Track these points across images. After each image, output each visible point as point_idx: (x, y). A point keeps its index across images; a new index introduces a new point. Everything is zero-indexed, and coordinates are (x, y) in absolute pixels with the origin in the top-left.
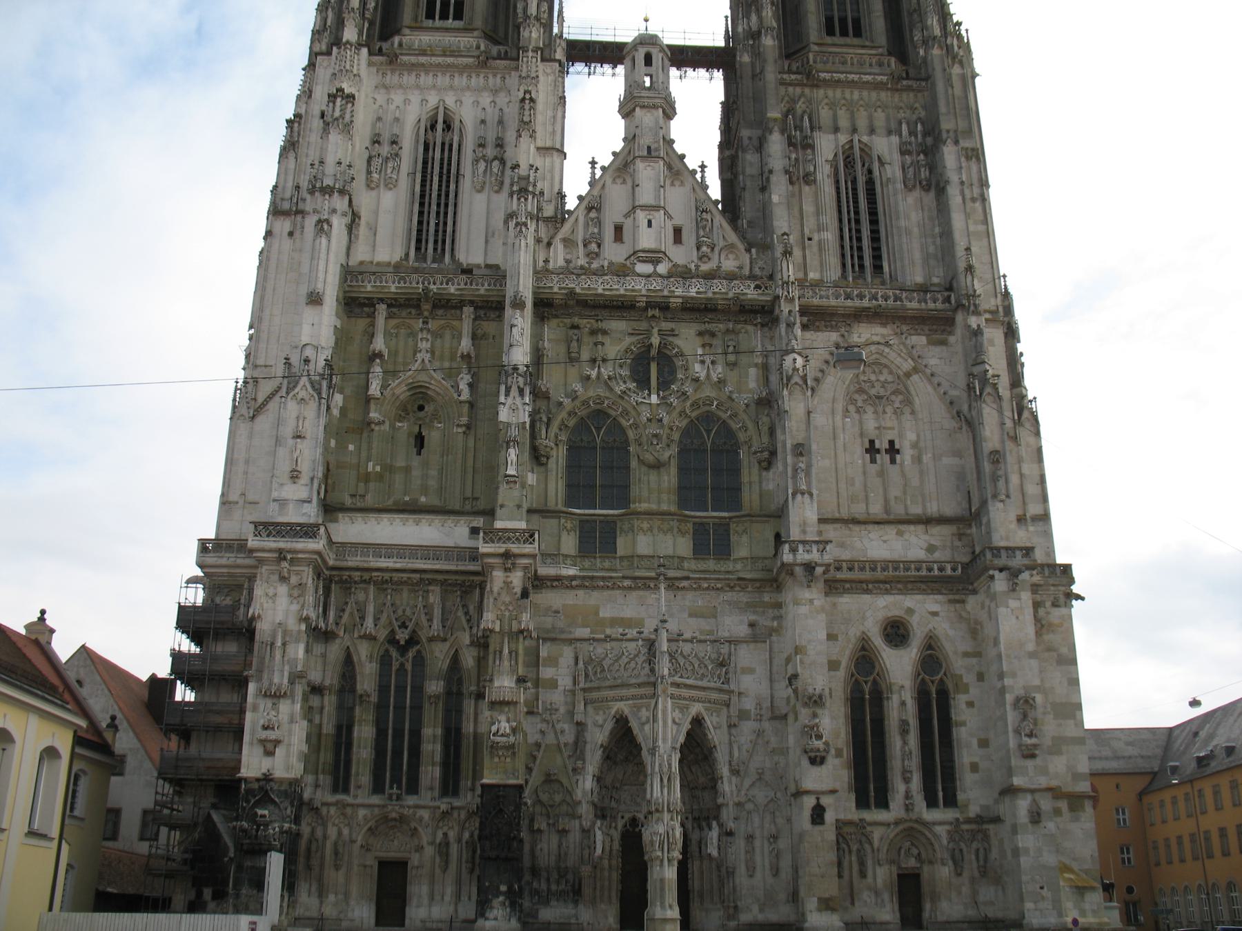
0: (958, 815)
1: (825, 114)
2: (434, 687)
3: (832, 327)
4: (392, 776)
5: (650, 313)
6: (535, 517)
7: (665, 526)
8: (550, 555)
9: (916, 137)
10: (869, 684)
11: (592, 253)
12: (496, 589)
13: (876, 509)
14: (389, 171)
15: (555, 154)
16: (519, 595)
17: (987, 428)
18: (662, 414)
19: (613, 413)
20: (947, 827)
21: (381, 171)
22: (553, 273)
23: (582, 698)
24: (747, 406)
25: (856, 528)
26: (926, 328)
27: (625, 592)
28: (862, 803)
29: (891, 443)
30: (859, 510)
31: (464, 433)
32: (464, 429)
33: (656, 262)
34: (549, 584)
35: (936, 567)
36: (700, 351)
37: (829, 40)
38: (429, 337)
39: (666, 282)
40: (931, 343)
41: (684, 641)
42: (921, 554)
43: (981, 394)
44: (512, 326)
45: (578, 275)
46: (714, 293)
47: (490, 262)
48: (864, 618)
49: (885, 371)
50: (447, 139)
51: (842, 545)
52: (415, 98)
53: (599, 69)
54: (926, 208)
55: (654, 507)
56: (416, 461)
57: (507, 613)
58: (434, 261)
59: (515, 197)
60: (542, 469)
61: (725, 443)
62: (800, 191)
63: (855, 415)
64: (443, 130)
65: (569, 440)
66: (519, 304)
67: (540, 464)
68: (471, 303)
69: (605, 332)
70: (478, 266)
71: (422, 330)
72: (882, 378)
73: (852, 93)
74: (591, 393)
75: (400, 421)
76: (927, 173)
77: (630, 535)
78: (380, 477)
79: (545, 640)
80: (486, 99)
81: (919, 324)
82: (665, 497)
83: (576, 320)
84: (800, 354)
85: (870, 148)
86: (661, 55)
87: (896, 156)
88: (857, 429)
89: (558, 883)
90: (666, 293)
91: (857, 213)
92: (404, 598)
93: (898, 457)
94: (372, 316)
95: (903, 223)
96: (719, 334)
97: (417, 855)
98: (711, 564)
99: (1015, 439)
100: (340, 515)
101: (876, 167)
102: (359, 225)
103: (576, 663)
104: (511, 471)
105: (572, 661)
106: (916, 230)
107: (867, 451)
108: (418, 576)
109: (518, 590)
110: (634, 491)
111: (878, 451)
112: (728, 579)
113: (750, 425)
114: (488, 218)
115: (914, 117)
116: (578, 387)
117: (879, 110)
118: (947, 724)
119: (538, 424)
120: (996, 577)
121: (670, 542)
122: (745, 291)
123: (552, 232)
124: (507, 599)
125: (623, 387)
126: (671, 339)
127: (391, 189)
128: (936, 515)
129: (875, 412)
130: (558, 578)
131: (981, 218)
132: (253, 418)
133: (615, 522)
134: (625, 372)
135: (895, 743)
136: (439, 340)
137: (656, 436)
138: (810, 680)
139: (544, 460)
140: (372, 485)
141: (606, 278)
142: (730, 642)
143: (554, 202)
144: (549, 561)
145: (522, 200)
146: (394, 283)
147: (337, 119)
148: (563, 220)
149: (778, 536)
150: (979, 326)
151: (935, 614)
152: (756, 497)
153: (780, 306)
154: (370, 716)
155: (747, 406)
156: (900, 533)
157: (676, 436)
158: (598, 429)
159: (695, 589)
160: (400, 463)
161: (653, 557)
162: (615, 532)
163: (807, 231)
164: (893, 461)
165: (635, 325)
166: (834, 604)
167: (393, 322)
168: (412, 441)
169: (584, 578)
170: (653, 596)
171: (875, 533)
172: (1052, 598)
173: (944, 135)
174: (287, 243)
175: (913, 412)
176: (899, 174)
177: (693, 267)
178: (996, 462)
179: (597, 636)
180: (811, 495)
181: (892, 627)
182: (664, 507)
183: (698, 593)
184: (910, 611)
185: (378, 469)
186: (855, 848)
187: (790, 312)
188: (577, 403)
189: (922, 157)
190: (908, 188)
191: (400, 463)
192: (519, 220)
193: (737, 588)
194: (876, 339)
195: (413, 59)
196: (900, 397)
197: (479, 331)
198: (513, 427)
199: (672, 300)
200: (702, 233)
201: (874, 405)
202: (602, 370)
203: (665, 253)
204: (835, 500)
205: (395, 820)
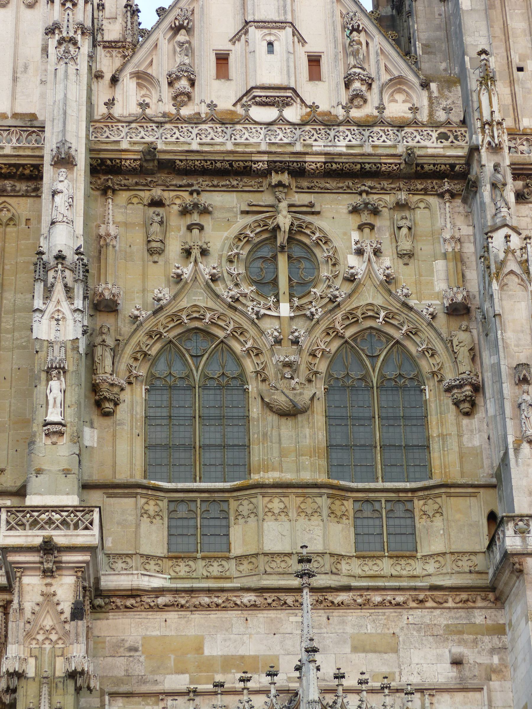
5: (275, 178)
7: (309, 506)
8: (120, 555)
11: (182, 94)
16: (67, 614)
19: (221, 334)
22: (119, 121)
24: (433, 316)
33: (285, 103)
34: (118, 601)
36: (355, 236)
39: (298, 132)
41: (347, 691)
44: (55, 193)
45: (160, 124)
47: (19, 110)
55: (289, 477)
57: (47, 646)
60: (107, 422)
67: (107, 414)
69: (205, 211)
74: (184, 303)
77: (252, 520)
79: (113, 695)
82: (306, 461)
83: (157, 192)
84: (514, 229)
90: (298, 148)
96: (385, 212)
104: (54, 416)
109: (67, 607)
112: (415, 589)
113: (439, 347)
114: (16, 45)
116: (166, 294)
119: (99, 349)
121: (318, 532)
122: (423, 143)
125: (235, 292)
126: (309, 218)
134: (239, 269)
137: (288, 365)
139: (108, 406)
141: (203, 126)
142: (422, 691)
143: (120, 20)
144: (120, 565)
148: (135, 46)
149: (492, 517)
152: (453, 457)
153: (479, 161)
157: (322, 367)
162: (227, 518)
169: (176, 591)
170: (293, 619)
177: (340, 113)
179: (201, 687)
182: (307, 477)
183: (365, 612)
187: (496, 168)
188: (162, 317)
192: (64, 34)
193: (430, 604)
197: (5, 212)
198: (56, 347)
199: (308, 159)
200: (352, 61)
202: (201, 266)
203: (294, 90)
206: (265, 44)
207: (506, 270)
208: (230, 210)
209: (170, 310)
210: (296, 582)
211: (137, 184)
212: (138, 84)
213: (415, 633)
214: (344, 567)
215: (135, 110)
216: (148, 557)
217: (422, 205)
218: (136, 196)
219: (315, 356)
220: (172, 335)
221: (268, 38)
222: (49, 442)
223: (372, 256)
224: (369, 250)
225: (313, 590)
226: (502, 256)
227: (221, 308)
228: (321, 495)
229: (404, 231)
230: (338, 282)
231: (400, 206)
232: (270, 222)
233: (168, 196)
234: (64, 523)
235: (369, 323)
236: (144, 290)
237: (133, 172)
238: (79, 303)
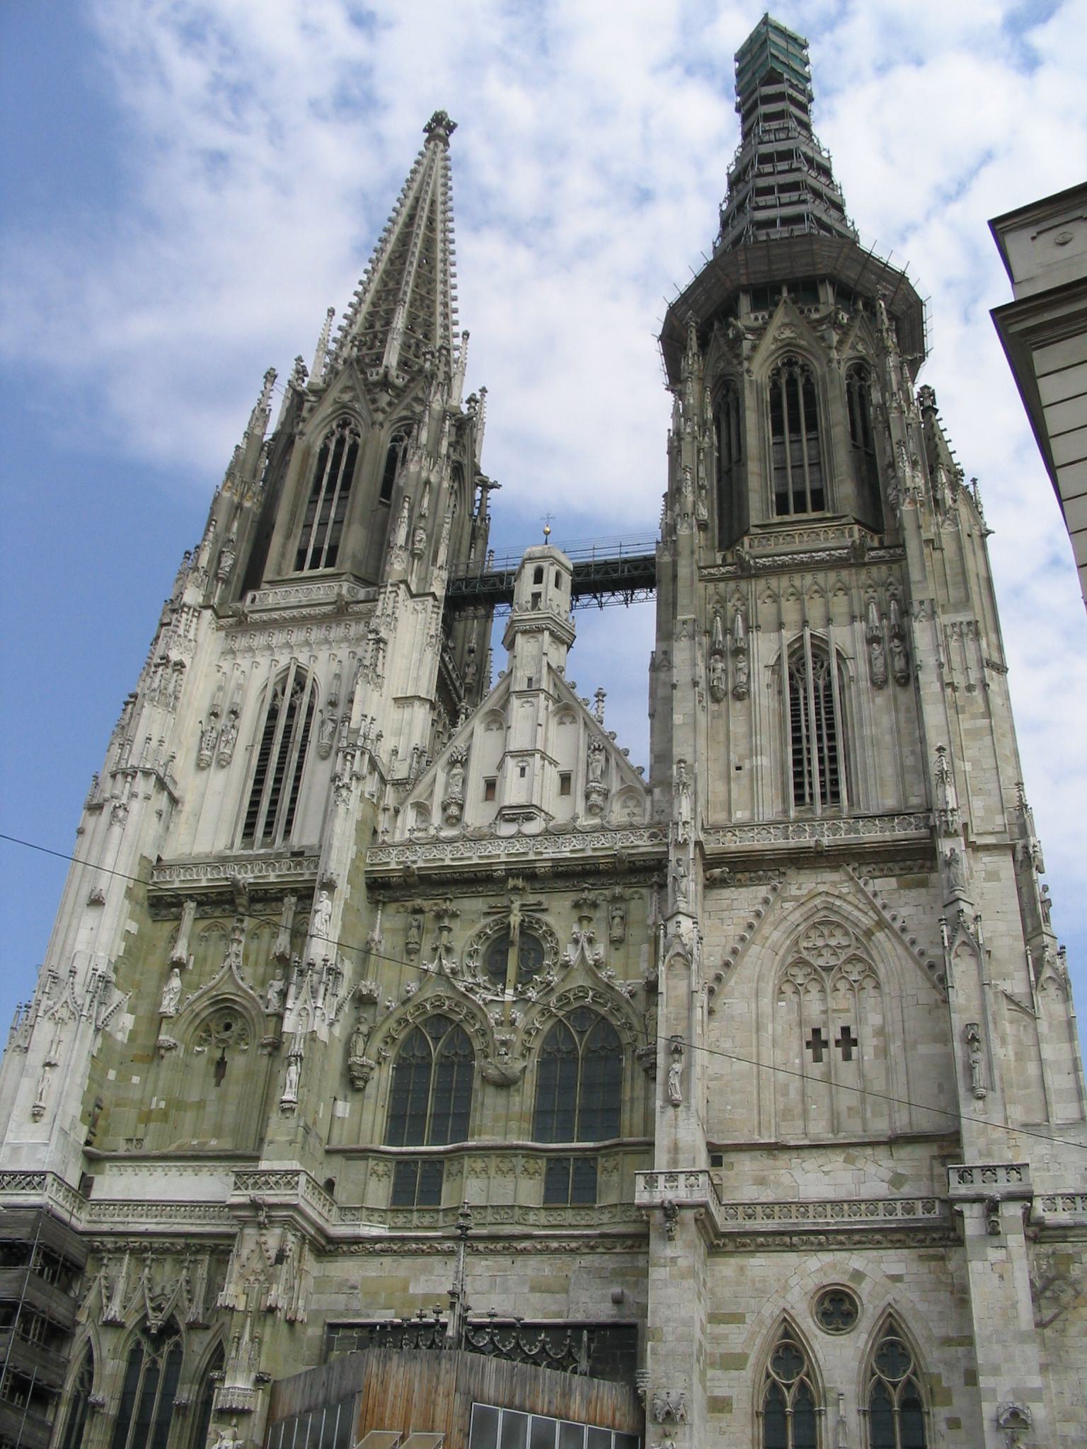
1: (765, 610)
3: (759, 879)
5: (511, 883)
6: (338, 1161)
9: (889, 619)
10: (793, 1390)
13: (819, 1129)
14: (223, 745)
15: (417, 703)
16: (273, 1260)
17: (960, 993)
18: (517, 1014)
19: (456, 1018)
21: (214, 747)
24: (633, 994)
25: (784, 1158)
27: (445, 1259)
29: (846, 1030)
31: (270, 1055)
32: (269, 1049)
33: (529, 818)
36: (576, 929)
38: (243, 939)
39: (533, 842)
40: (904, 886)
42: (882, 1190)
43: (951, 943)
46: (594, 850)
48: (786, 1288)
49: (838, 933)
51: (761, 1182)
52: (264, 660)
54: (903, 708)
58: (263, 845)
59: (340, 755)
60: (360, 1096)
61: (603, 1048)
63: (792, 996)
65: (399, 1057)
72: (833, 942)
73: (803, 579)
74: (429, 994)
75: (200, 1045)
76: (903, 662)
77: (458, 1179)
78: (164, 1115)
80: (343, 652)
81: (885, 862)
87: (861, 648)
94: (178, 918)
95: (867, 731)
98: (569, 1216)
100: (108, 1165)
102: (181, 811)
104: (289, 1096)
106: (888, 738)
107: (808, 1044)
108: (183, 1240)
109: (273, 1253)
110: (475, 1120)
111: (825, 1044)
112: (587, 1236)
116: (413, 987)
117: (841, 593)
120: (966, 1214)
122: (636, 843)
123: (403, 795)
124: (258, 1266)
126: (538, 915)
127: (223, 767)
129: (822, 991)
130: (357, 1240)
131: (982, 709)
133: (442, 1162)
134: (477, 963)
136: (255, 941)
137: (504, 1043)
139: (360, 1083)
140: (152, 1125)
143: (409, 760)
145: (349, 757)
146: (205, 875)
147: (154, 690)
150: (953, 850)
151: (897, 1278)
155: (633, 994)
157: (536, 1044)
158: (436, 1039)
159: (540, 1252)
161: (485, 1207)
163: (734, 760)
164: (847, 1057)
165: (493, 901)
166: (742, 1268)
167: (206, 922)
168: (212, 1069)
170: (483, 1263)
171: (812, 1162)
173: (916, 608)
175: (877, 986)
176: (863, 668)
178: (972, 1041)
180: (688, 1108)
181: (832, 1300)
183: (544, 1257)
184: (858, 1276)
185: (163, 1105)
189: (896, 641)
191: (194, 1097)
194: (822, 888)
195: (265, 616)
196: (860, 967)
198: (298, 1039)
201: (819, 980)
202: (444, 962)
204: (756, 1117)
206: (519, 769)
211: (404, 896)
212: (418, 812)
213: (585, 1276)
214: (532, 1218)
216: (373, 1210)
217: (636, 896)
218: (403, 906)
219: (530, 1034)
220: (417, 1021)
221: (521, 764)
223: (586, 945)
224: (583, 940)
228: (516, 1156)
229: (617, 920)
232: (505, 921)
233: (426, 904)
236: (399, 985)
237: (399, 886)
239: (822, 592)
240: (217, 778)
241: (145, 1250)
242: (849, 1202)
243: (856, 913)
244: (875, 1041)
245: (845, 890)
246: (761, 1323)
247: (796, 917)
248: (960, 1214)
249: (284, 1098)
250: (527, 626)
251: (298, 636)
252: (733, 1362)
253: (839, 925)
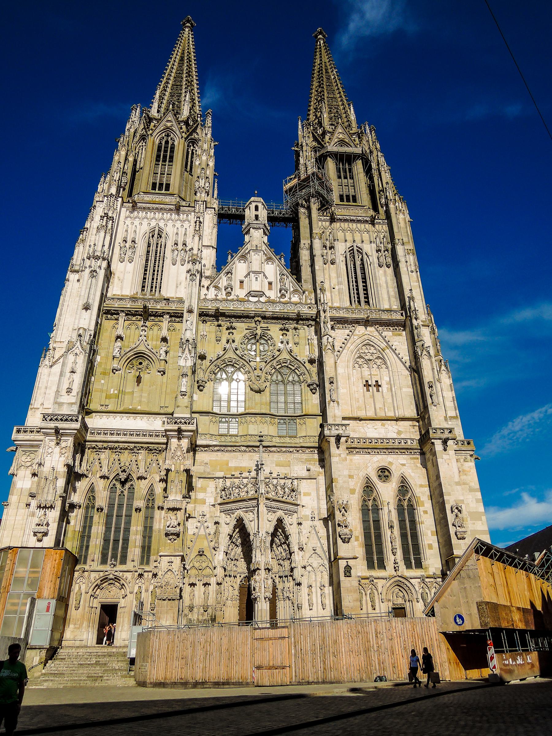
0: (423, 574)
1: (340, 235)
2: (139, 503)
4: (112, 554)
5: (256, 319)
7: (264, 420)
11: (229, 293)
12: (173, 449)
13: (371, 414)
16: (185, 451)
19: (238, 366)
20: (419, 580)
23: (218, 509)
26: (391, 328)
28: (370, 566)
29: (377, 381)
30: (362, 414)
35: (402, 441)
36: (281, 337)
37: (341, 203)
42: (395, 436)
44: (187, 321)
48: (367, 467)
49: (372, 348)
50: (160, 241)
52: (145, 222)
53: (235, 222)
56: (136, 389)
62: (329, 267)
64: (158, 238)
66: (190, 311)
67: (201, 391)
68: (168, 313)
69: (234, 329)
70: (173, 298)
71: (142, 326)
75: (129, 370)
80: (178, 224)
85: (362, 250)
86: (263, 206)
87: (374, 252)
88: (359, 375)
89: (203, 615)
91: (356, 278)
92: (126, 457)
93: (380, 388)
96: (290, 330)
97: (123, 600)
99: (439, 381)
101: (365, 256)
103: (216, 491)
105: (214, 490)
109: (185, 449)
111: (370, 386)
114: (177, 277)
115: (382, 236)
116: (222, 353)
118: (413, 522)
121: (266, 428)
126: (267, 331)
128: (401, 416)
132: (51, 366)
135: (387, 533)
136: (151, 331)
138: (340, 496)
144: (203, 437)
147: (104, 226)
151: (403, 465)
154: (103, 520)
156: (383, 425)
160: (129, 390)
163: (333, 286)
169: (221, 446)
172: (463, 457)
174: (77, 285)
175: (387, 368)
176: (376, 260)
179: (227, 476)
181: (381, 472)
182: (263, 411)
184: (390, 463)
185: (116, 392)
186: (368, 593)
190: (380, 266)
191: (129, 390)
193: (301, 452)
195: (144, 205)
196: (380, 360)
198: (185, 368)
205: (112, 579)
207: (327, 348)
208: (242, 328)
209: (223, 358)
210: (258, 444)
214: (274, 439)
215: (214, 297)
222: (181, 397)
225: (264, 447)
226: (326, 344)
227: (238, 358)
230: (275, 351)
231: (296, 329)
234: (185, 423)
235: (285, 364)
238: (193, 355)
239: (360, 231)
240: (130, 267)
241: (116, 448)
242: (386, 439)
243: (379, 342)
244: (387, 386)
245: (375, 334)
246: (359, 478)
247: (359, 341)
248: (433, 443)
249: (182, 390)
250: (255, 226)
251: (158, 215)
252: (353, 491)
253: (373, 346)
